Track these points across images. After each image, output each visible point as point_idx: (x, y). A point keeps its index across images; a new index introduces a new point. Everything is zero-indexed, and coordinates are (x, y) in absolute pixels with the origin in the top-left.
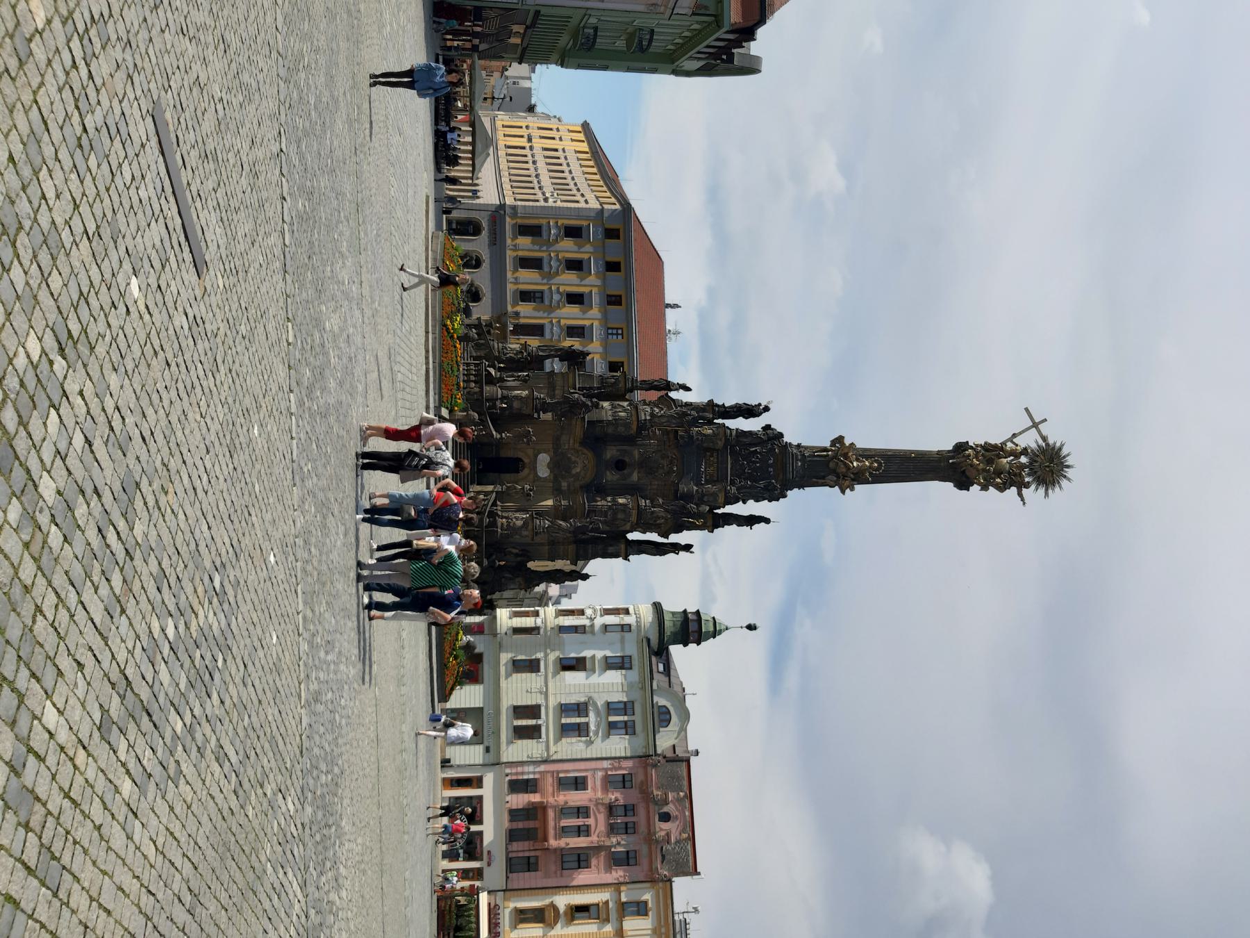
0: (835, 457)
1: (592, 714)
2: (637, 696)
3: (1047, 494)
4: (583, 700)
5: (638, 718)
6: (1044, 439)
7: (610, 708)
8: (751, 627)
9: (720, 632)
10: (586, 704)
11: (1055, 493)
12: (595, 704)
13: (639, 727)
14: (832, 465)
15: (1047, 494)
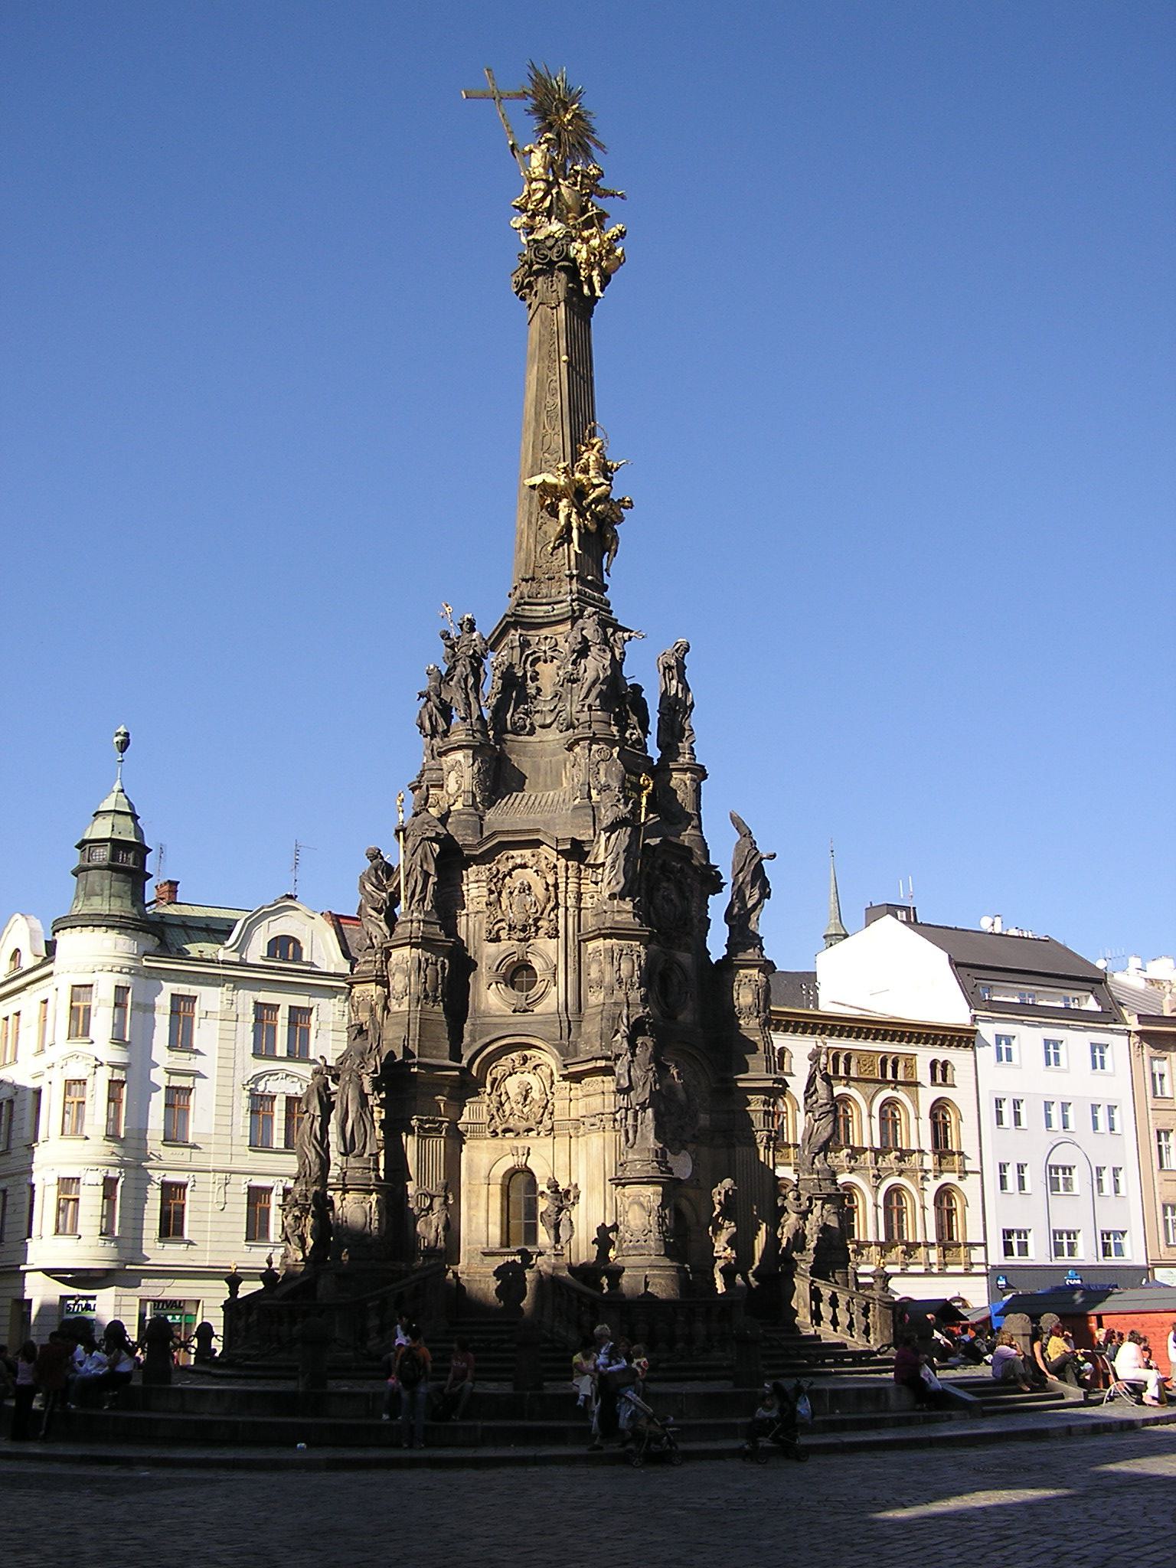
0: (581, 514)
1: (271, 1086)
2: (247, 999)
3: (598, 145)
4: (245, 1103)
5: (285, 1001)
6: (524, 95)
7: (263, 1050)
8: (124, 745)
9: (131, 805)
10: (253, 1095)
11: (603, 128)
12: (257, 1079)
13: (301, 1001)
14: (592, 527)
15: (598, 145)
